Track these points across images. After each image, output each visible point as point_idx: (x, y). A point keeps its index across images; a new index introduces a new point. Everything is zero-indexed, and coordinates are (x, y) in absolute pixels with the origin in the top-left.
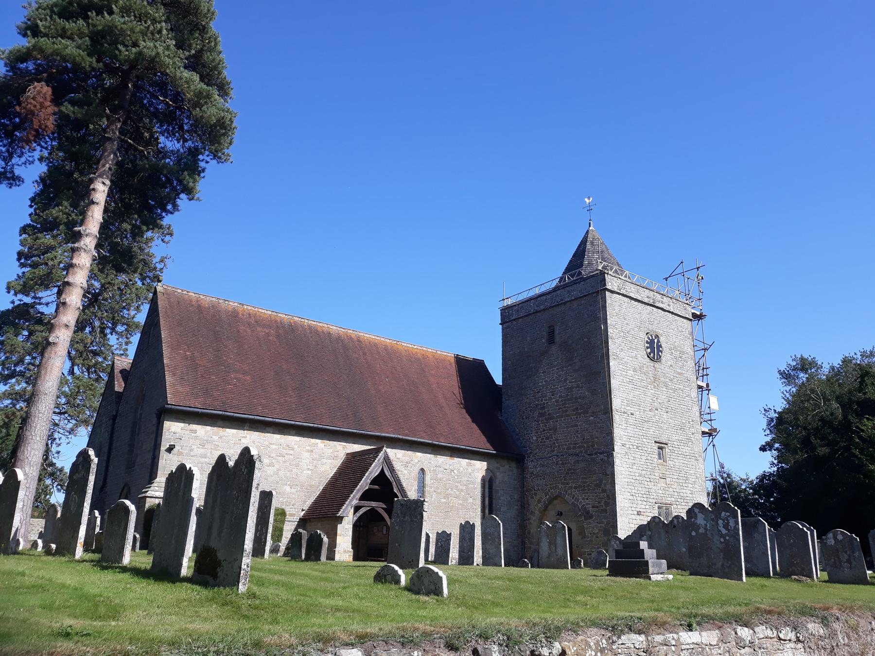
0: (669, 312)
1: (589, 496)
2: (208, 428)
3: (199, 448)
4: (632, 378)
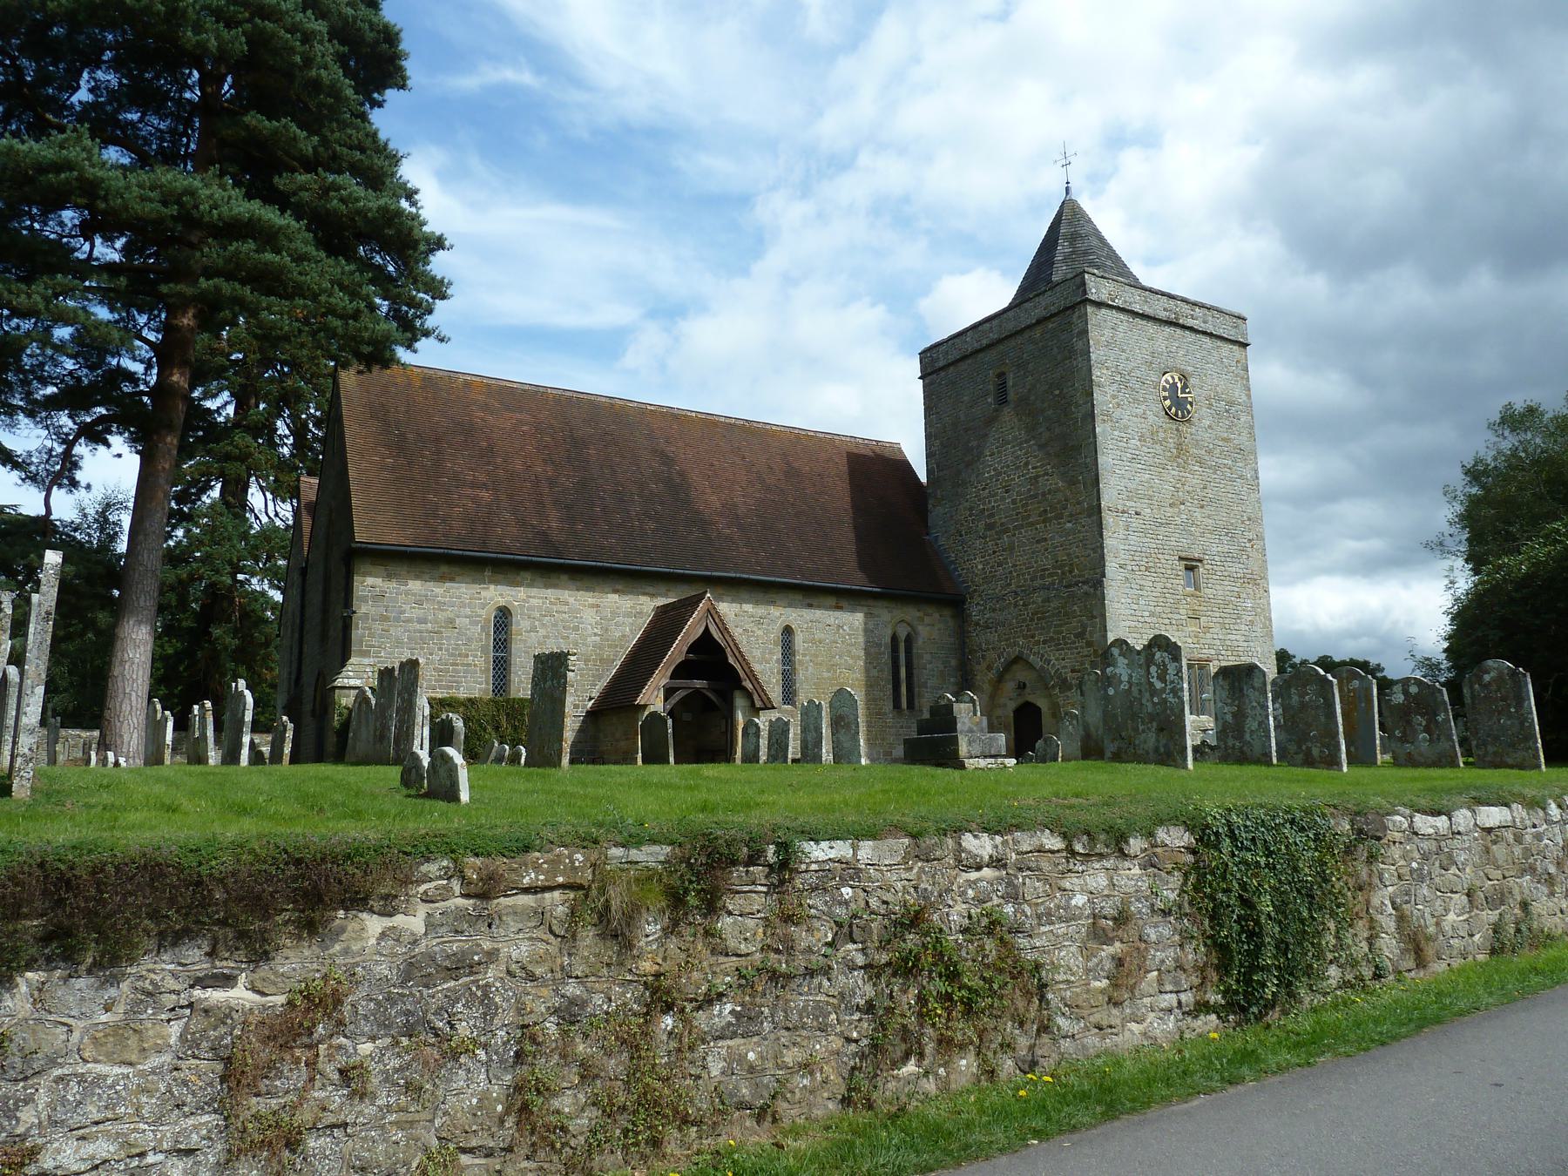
0: (1204, 333)
3: (414, 608)
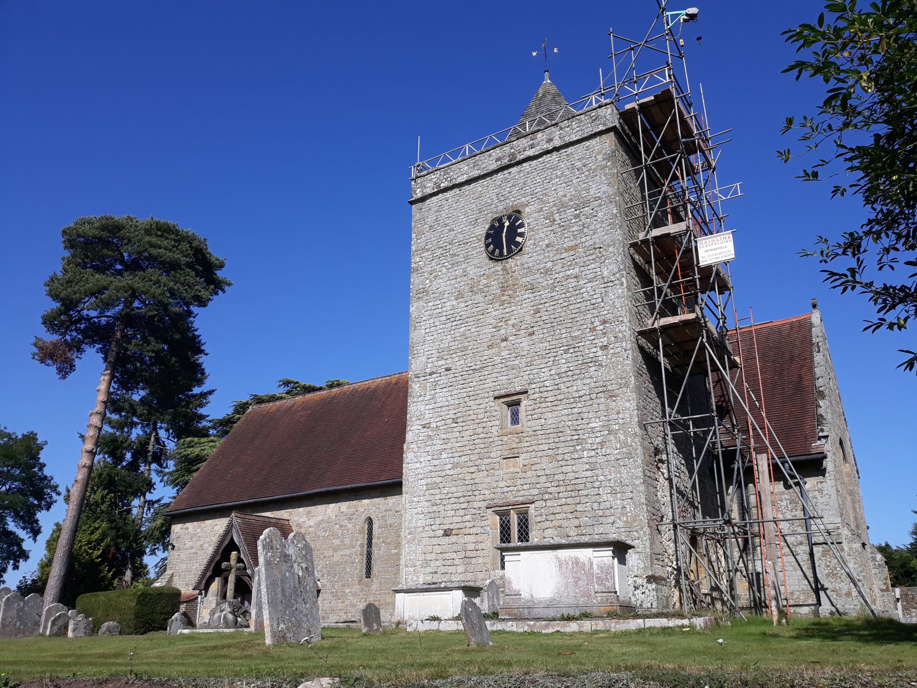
2: (195, 523)
4: (452, 312)
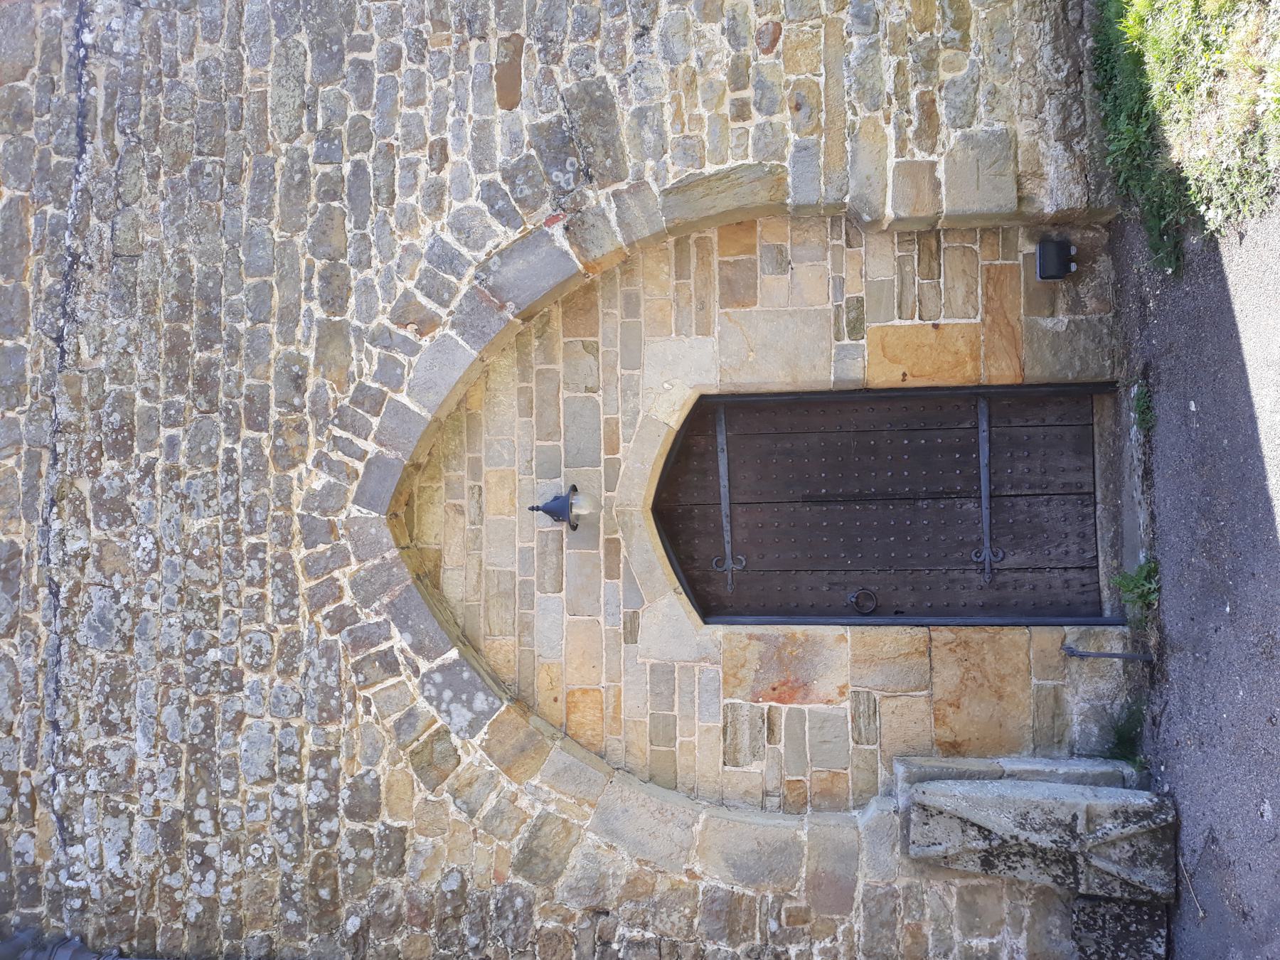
1: (413, 124)
